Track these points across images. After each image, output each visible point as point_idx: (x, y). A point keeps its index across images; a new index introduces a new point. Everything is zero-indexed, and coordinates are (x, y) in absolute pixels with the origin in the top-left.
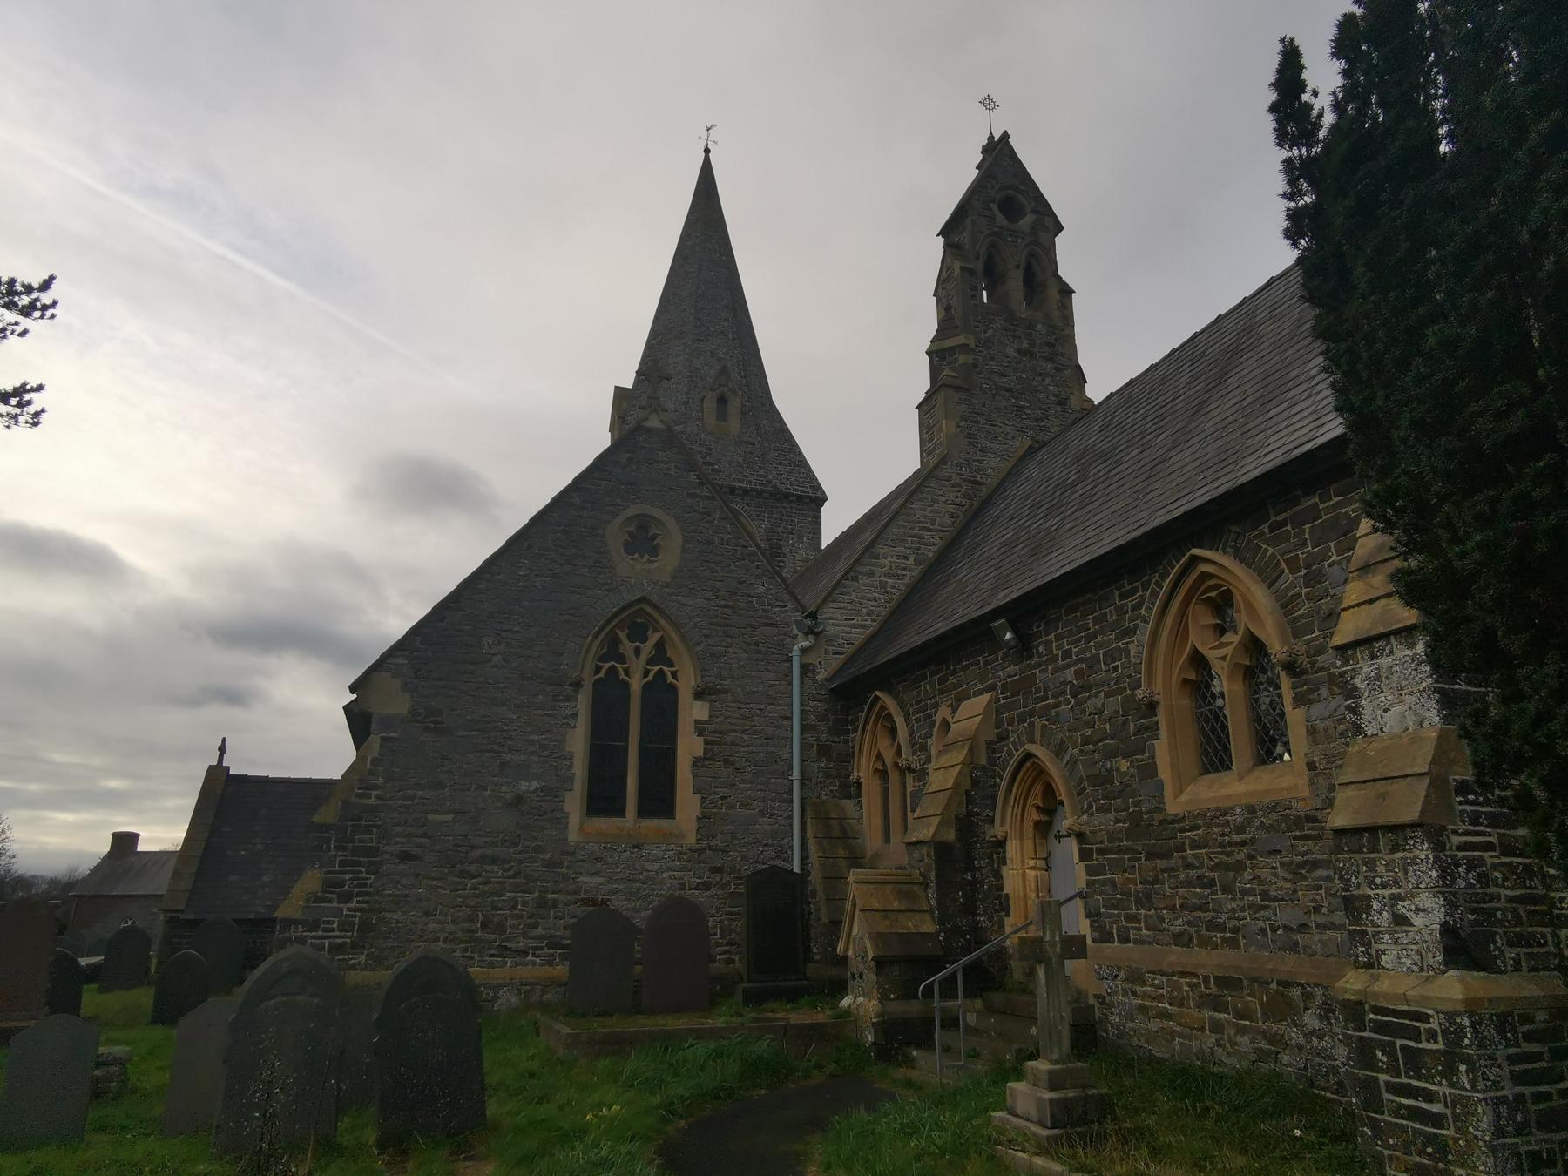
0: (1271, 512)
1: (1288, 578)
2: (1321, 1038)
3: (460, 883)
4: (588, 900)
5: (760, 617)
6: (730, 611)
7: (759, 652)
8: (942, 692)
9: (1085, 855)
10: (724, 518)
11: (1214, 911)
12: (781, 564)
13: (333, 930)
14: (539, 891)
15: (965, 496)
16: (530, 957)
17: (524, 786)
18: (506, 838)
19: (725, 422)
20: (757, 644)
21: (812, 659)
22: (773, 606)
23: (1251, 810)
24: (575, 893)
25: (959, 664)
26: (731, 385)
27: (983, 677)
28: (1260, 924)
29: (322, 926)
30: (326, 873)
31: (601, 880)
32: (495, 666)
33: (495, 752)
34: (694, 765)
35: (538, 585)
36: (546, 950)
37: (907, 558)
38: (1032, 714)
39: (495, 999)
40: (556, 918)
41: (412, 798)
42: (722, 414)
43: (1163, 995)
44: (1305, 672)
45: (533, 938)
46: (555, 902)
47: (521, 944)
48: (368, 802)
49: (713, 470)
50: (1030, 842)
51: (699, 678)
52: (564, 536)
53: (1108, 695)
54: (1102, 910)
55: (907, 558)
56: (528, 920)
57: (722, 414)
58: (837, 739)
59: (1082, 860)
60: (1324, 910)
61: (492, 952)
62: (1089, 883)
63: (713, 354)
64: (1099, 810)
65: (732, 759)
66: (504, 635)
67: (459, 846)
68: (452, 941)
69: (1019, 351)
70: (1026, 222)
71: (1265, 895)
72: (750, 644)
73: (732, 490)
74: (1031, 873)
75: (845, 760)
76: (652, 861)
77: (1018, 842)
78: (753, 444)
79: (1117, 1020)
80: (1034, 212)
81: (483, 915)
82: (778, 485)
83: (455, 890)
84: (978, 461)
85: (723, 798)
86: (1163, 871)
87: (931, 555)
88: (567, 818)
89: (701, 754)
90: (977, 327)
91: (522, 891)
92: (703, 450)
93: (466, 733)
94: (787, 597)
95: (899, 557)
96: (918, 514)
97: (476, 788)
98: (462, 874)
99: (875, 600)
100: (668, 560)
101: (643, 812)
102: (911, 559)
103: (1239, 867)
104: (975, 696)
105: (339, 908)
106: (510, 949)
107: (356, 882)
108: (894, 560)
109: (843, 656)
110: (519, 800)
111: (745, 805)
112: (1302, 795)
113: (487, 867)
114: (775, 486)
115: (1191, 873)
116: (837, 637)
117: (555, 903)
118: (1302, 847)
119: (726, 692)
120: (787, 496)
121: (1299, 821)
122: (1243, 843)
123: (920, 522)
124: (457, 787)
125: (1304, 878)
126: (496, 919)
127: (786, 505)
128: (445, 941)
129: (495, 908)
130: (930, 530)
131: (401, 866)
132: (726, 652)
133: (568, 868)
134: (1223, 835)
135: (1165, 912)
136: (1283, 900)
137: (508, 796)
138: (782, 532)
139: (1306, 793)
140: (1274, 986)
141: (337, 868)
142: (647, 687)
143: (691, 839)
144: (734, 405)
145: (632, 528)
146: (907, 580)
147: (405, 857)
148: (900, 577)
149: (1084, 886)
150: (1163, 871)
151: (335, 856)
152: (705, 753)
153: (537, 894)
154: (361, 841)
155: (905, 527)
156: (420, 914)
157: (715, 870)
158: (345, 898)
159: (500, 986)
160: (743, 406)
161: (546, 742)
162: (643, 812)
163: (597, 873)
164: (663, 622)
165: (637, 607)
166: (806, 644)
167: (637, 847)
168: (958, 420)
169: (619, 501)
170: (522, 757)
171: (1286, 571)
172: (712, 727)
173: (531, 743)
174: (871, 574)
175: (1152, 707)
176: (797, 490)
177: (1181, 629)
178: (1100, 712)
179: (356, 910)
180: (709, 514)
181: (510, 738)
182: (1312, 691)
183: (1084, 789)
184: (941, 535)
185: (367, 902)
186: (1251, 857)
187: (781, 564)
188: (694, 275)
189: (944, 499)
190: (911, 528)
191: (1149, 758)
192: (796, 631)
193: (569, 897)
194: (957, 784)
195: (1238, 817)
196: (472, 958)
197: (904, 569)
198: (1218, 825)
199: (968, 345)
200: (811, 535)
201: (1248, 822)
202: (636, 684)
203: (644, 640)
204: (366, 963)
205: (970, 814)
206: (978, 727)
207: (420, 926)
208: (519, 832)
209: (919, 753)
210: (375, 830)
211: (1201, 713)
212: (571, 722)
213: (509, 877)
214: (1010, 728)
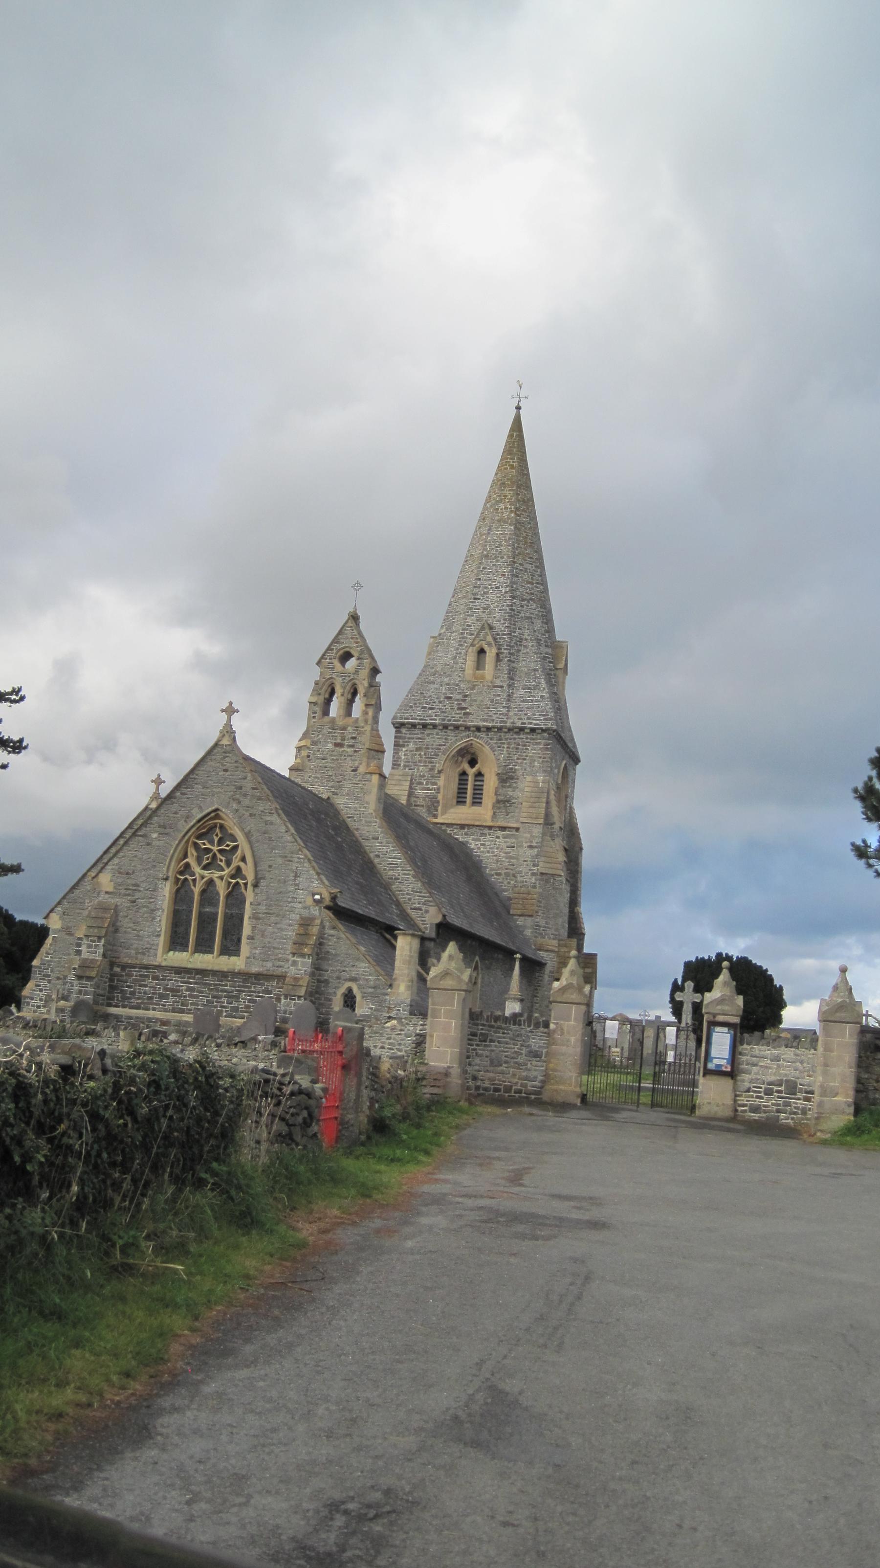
12: (515, 785)
42: (479, 664)
57: (479, 664)
73: (478, 729)
120: (522, 729)
138: (518, 759)
176: (531, 723)
187: (515, 785)
200: (541, 760)
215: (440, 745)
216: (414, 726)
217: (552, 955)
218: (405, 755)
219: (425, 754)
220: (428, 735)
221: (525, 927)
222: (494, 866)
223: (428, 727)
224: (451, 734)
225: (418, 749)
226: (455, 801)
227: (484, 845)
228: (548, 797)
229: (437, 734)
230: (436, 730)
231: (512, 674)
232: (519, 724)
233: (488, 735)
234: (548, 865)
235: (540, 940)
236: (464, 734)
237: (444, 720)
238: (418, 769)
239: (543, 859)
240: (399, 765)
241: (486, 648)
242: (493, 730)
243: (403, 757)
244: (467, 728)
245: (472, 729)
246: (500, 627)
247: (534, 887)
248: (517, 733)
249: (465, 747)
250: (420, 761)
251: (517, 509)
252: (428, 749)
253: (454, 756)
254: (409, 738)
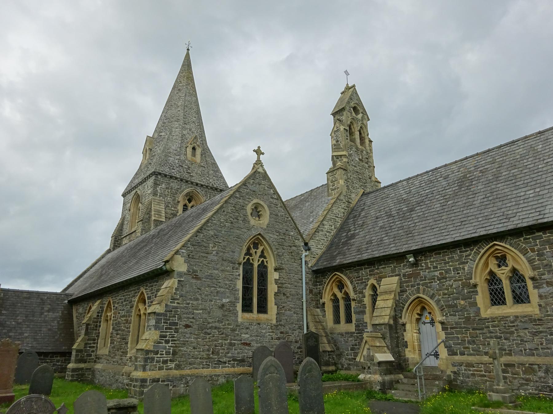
0: (524, 235)
1: (530, 254)
2: (544, 378)
3: (205, 337)
4: (244, 343)
5: (292, 243)
6: (284, 240)
7: (292, 256)
8: (371, 275)
9: (443, 329)
10: (281, 207)
11: (501, 345)
13: (163, 354)
14: (230, 340)
15: (347, 207)
16: (227, 365)
17: (224, 301)
18: (219, 320)
19: (195, 157)
20: (291, 253)
21: (308, 260)
22: (296, 240)
23: (517, 317)
24: (241, 341)
25: (380, 266)
26: (198, 143)
27: (393, 271)
28: (520, 348)
29: (160, 353)
30: (161, 332)
31: (248, 336)
32: (214, 255)
33: (215, 287)
34: (275, 295)
35: (227, 225)
36: (232, 362)
37: (332, 226)
38: (418, 284)
39: (218, 380)
40: (235, 350)
41: (188, 304)
42: (194, 155)
43: (482, 370)
44: (537, 280)
45: (228, 357)
46: (235, 344)
47: (224, 360)
48: (174, 305)
49: (190, 176)
50: (414, 325)
51: (276, 263)
52: (234, 208)
53: (455, 281)
54: (453, 346)
55: (332, 226)
56: (227, 351)
57: (194, 155)
58: (314, 288)
59: (443, 330)
60: (544, 344)
61: (215, 362)
62: (446, 338)
63: (190, 130)
64: (450, 315)
65: (286, 293)
66: (216, 243)
67: (204, 322)
68: (202, 359)
69: (359, 159)
70: (360, 116)
71: (522, 340)
72: (290, 253)
73: (197, 184)
74: (415, 334)
75: (320, 294)
76: (263, 329)
77: (410, 324)
78: (204, 167)
79: (462, 378)
80: (362, 113)
81: (212, 349)
82: (214, 185)
83: (204, 339)
84: (350, 195)
85: (283, 307)
86: (480, 334)
87: (338, 226)
88: (238, 313)
89: (277, 291)
90: (348, 149)
91: (224, 340)
92: (186, 167)
93: (206, 280)
94: (300, 237)
95: (330, 226)
96: (335, 211)
97: (209, 301)
98: (206, 333)
99: (324, 240)
100: (265, 220)
101: (259, 312)
102: (333, 226)
103: (512, 333)
104: (389, 277)
105: (165, 346)
106: (221, 361)
107: (171, 336)
108: (328, 226)
109: (315, 259)
110: (223, 305)
111: (289, 310)
112: (537, 313)
113: (213, 331)
114: (212, 185)
115: (492, 334)
116: (314, 252)
117: (234, 344)
118: (536, 327)
119: (283, 269)
120: (216, 189)
121: (535, 320)
122: (514, 326)
123: (335, 214)
124: (203, 300)
125: (537, 336)
126: (217, 350)
127: (216, 192)
128: (200, 359)
129: (216, 346)
130: (338, 217)
131: (185, 330)
132: (283, 255)
133: (238, 331)
134: (505, 323)
135: (481, 346)
136: (529, 342)
137: (219, 304)
139: (538, 312)
140: (527, 365)
141: (164, 330)
142: (259, 266)
143: (274, 322)
144: (199, 151)
145: (253, 208)
146: (332, 234)
147: (187, 326)
148: (330, 233)
149: (445, 338)
150: (480, 334)
151: (164, 326)
152: (278, 291)
153: (229, 341)
154: (172, 320)
155: (331, 215)
156: (192, 348)
157: (281, 333)
158: (167, 342)
159: (219, 375)
160: (202, 152)
161: (231, 285)
162: (259, 312)
163: (247, 333)
164: (265, 243)
165: (257, 237)
166: (307, 254)
167: (259, 324)
168: (344, 180)
169: (250, 197)
170: (223, 290)
171: (530, 252)
172: (279, 281)
173: (226, 284)
174: (322, 231)
175: (475, 286)
176: (220, 187)
177: (486, 264)
178: (452, 286)
179: (171, 347)
180: (277, 205)
181: (220, 282)
182: (540, 285)
183: (444, 309)
184: (341, 219)
185: (175, 344)
186: (516, 330)
188: (183, 98)
189: (341, 207)
190: (333, 216)
191: (474, 301)
192: (302, 249)
193: (239, 342)
194: (393, 305)
195: (512, 318)
196: (209, 365)
197: (331, 230)
198: (502, 321)
199: (346, 155)
201: (516, 320)
202: (256, 264)
203: (257, 249)
204: (175, 367)
205: (396, 315)
206: (396, 288)
207: (192, 353)
208: (223, 318)
209: (358, 294)
210: (177, 316)
211: (490, 289)
212: (238, 277)
213: (220, 335)
214: (407, 288)
215: (179, 189)
216: (166, 176)
218: (160, 190)
219: (171, 192)
220: (172, 182)
223: (173, 178)
224: (184, 185)
225: (167, 188)
229: (177, 183)
230: (176, 181)
233: (201, 188)
236: (189, 185)
237: (181, 176)
238: (167, 199)
240: (157, 195)
241: (197, 147)
242: (204, 186)
243: (159, 191)
244: (192, 183)
245: (194, 184)
248: (213, 190)
249: (190, 192)
250: (168, 195)
252: (172, 189)
254: (162, 182)
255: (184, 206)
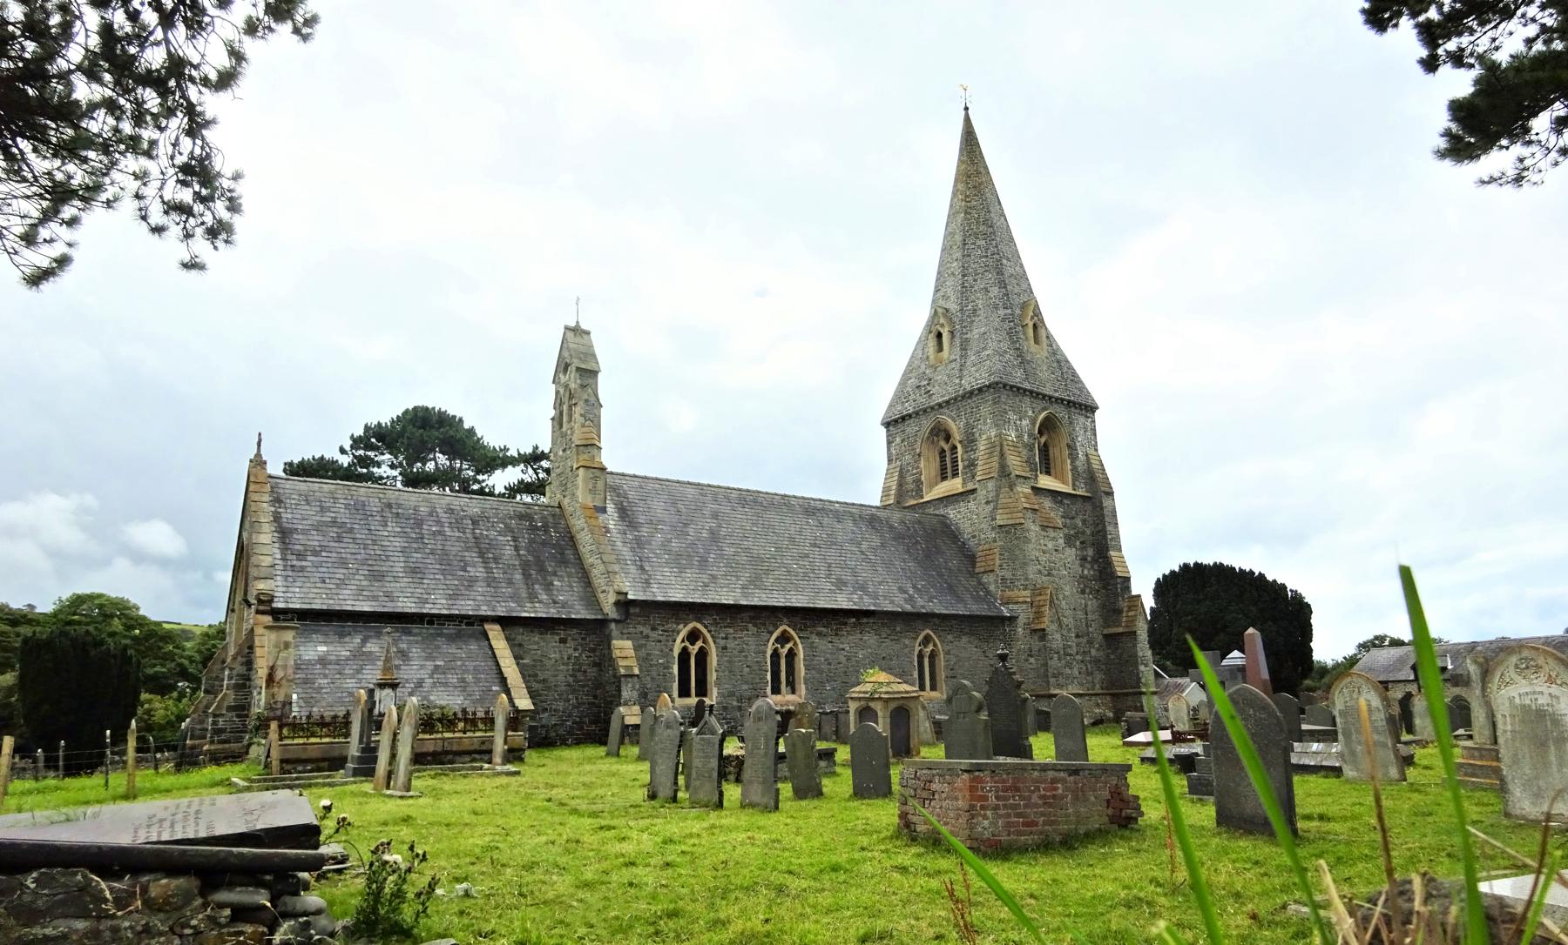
57: (940, 349)
73: (940, 405)
216: (896, 421)
217: (1024, 606)
221: (989, 583)
222: (970, 530)
226: (939, 478)
227: (959, 512)
228: (1001, 450)
231: (964, 348)
232: (969, 389)
234: (1005, 516)
235: (1008, 593)
239: (1000, 511)
244: (932, 408)
246: (953, 307)
247: (995, 541)
251: (967, 196)
253: (928, 438)
255: (940, 454)
